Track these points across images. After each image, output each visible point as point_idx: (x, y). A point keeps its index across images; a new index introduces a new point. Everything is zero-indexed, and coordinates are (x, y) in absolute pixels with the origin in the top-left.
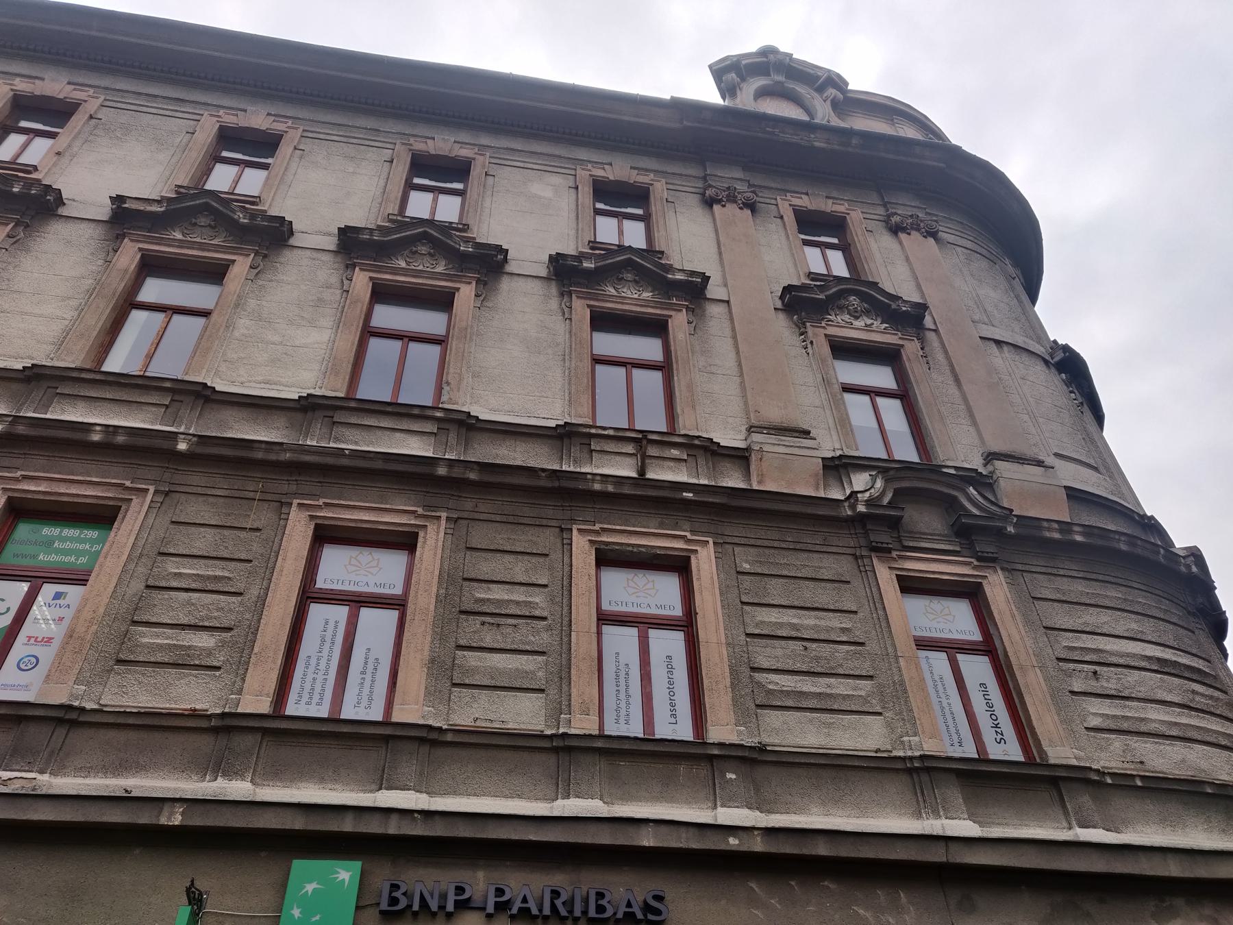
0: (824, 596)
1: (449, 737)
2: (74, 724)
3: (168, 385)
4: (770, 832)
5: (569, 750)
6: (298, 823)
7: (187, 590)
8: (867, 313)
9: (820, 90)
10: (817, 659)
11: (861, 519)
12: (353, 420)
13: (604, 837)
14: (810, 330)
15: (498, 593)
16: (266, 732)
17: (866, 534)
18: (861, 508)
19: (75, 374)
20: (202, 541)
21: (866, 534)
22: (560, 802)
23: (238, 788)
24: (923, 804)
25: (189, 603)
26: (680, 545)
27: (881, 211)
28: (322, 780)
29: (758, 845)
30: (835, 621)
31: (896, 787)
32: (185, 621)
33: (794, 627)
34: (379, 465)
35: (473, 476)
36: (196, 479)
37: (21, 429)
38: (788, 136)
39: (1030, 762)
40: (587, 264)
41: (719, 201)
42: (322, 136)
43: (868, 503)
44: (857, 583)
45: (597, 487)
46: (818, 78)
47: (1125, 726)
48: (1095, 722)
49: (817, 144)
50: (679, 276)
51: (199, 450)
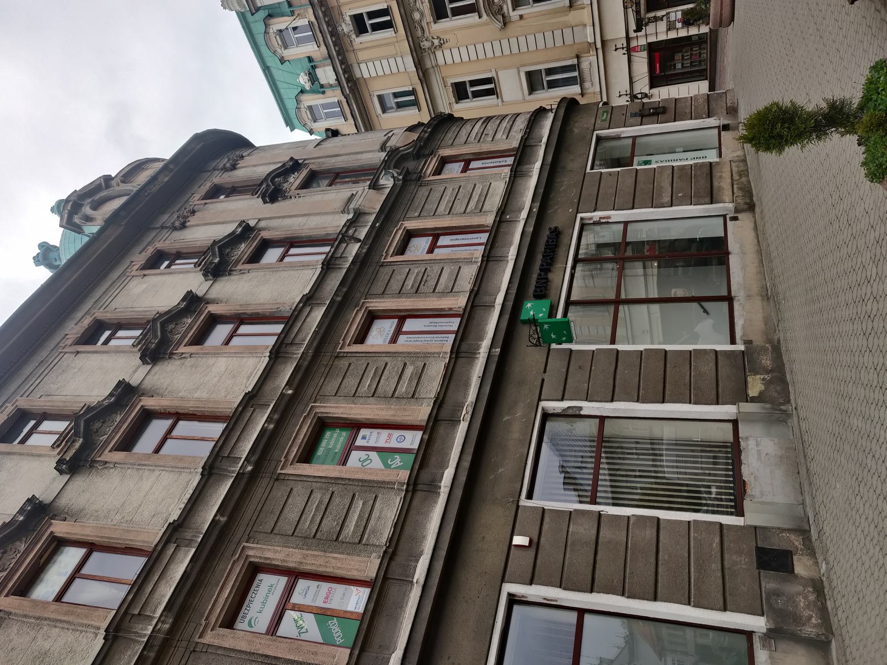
0: (435, 196)
1: (476, 289)
2: (442, 402)
3: (240, 409)
4: (533, 201)
5: (488, 257)
6: (507, 317)
7: (379, 382)
8: (285, 178)
9: (108, 186)
10: (464, 197)
11: (404, 179)
12: (293, 336)
13: (528, 240)
14: (290, 194)
15: (410, 283)
16: (462, 340)
17: (411, 180)
18: (401, 177)
19: (217, 449)
20: (351, 383)
21: (411, 180)
22: (510, 257)
23: (486, 344)
24: (527, 175)
25: (387, 380)
26: (401, 232)
27: (217, 172)
28: (486, 324)
29: (537, 204)
30: (449, 192)
31: (519, 181)
32: (396, 379)
33: (449, 202)
34: (327, 320)
35: (345, 289)
36: (310, 391)
37: (254, 458)
38: (155, 189)
39: (515, 156)
40: (217, 260)
41: (185, 222)
42: (31, 388)
43: (399, 174)
44: (432, 186)
45: (364, 251)
46: (100, 185)
47: (507, 131)
48: (504, 137)
49: (166, 179)
50: (239, 230)
51: (295, 386)
